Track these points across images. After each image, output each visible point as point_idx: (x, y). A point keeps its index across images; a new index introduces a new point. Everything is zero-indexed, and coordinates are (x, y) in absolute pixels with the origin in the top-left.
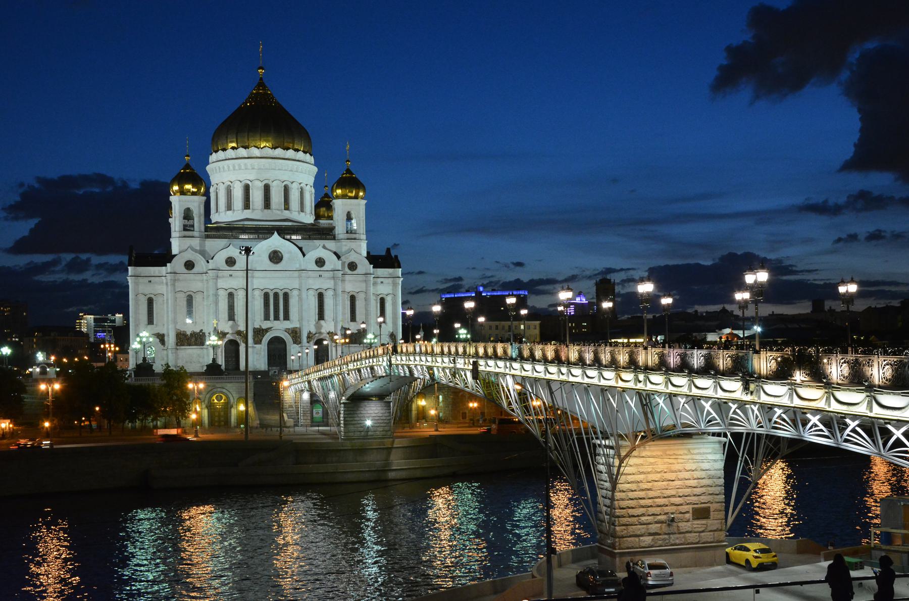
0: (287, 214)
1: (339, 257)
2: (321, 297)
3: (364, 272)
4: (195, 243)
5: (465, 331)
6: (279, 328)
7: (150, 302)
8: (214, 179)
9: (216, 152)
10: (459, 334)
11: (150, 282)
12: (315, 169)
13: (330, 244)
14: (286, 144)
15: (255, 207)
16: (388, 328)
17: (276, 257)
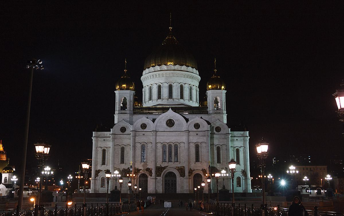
0: (182, 101)
1: (209, 123)
2: (197, 147)
3: (225, 133)
4: (127, 117)
5: (294, 168)
6: (172, 166)
7: (104, 151)
8: (145, 84)
9: (145, 70)
10: (289, 170)
11: (104, 140)
12: (199, 78)
13: (205, 117)
14: (181, 63)
15: (164, 98)
16: (242, 167)
17: (170, 123)
